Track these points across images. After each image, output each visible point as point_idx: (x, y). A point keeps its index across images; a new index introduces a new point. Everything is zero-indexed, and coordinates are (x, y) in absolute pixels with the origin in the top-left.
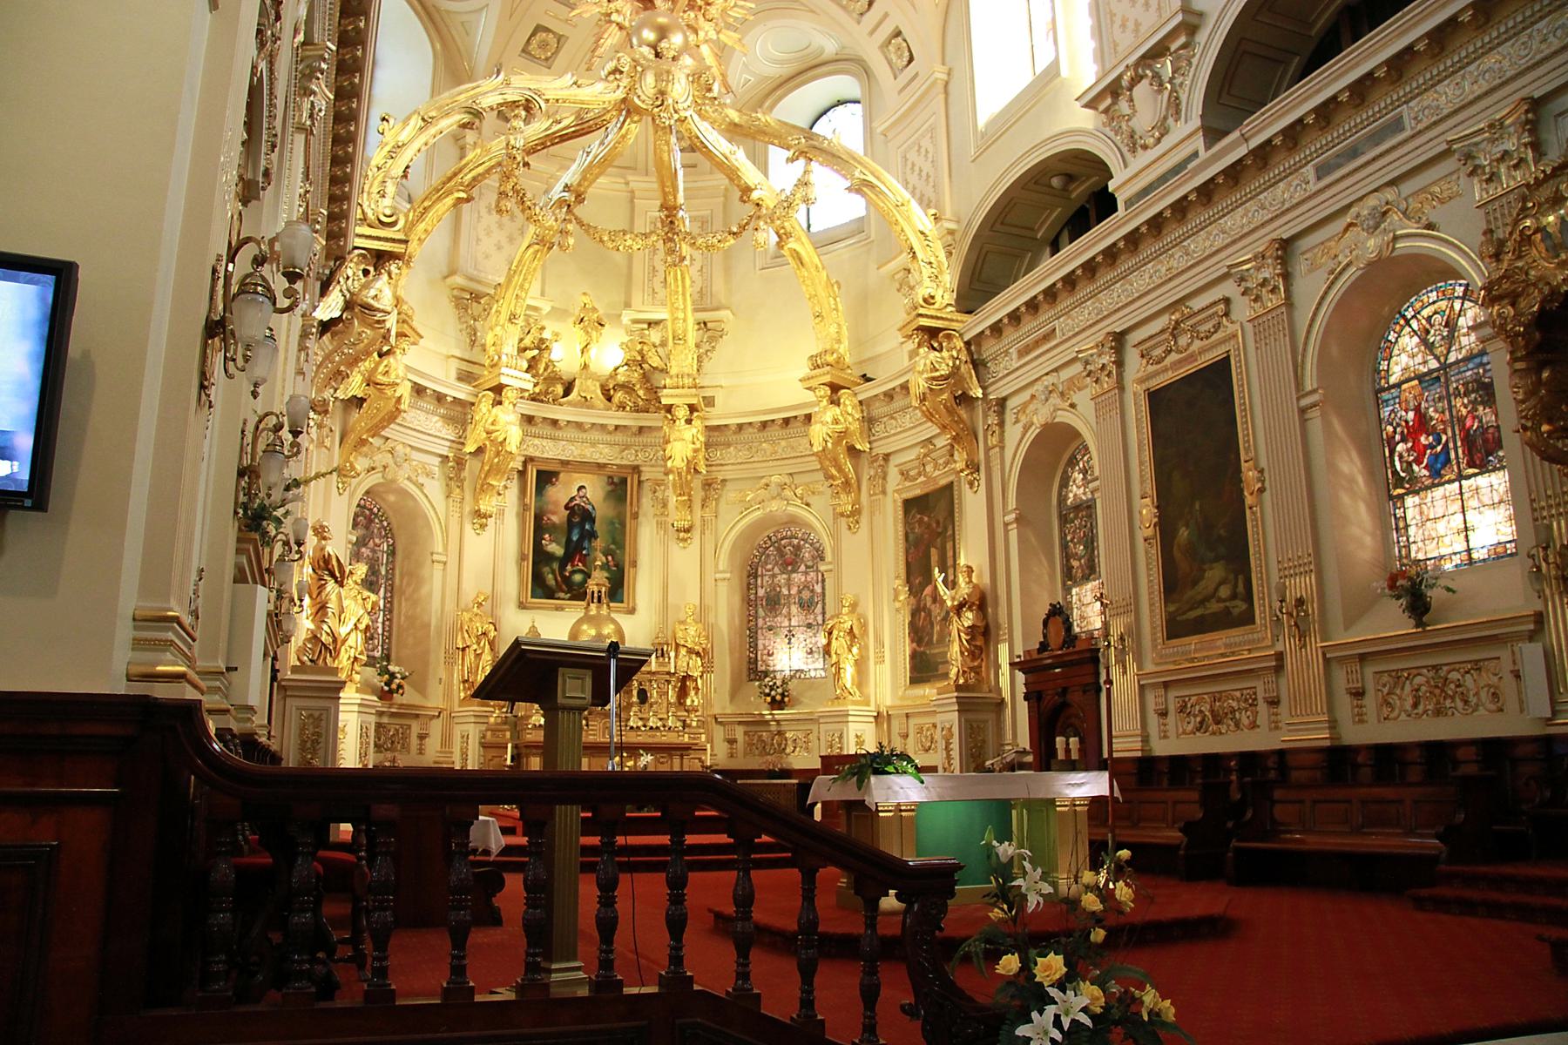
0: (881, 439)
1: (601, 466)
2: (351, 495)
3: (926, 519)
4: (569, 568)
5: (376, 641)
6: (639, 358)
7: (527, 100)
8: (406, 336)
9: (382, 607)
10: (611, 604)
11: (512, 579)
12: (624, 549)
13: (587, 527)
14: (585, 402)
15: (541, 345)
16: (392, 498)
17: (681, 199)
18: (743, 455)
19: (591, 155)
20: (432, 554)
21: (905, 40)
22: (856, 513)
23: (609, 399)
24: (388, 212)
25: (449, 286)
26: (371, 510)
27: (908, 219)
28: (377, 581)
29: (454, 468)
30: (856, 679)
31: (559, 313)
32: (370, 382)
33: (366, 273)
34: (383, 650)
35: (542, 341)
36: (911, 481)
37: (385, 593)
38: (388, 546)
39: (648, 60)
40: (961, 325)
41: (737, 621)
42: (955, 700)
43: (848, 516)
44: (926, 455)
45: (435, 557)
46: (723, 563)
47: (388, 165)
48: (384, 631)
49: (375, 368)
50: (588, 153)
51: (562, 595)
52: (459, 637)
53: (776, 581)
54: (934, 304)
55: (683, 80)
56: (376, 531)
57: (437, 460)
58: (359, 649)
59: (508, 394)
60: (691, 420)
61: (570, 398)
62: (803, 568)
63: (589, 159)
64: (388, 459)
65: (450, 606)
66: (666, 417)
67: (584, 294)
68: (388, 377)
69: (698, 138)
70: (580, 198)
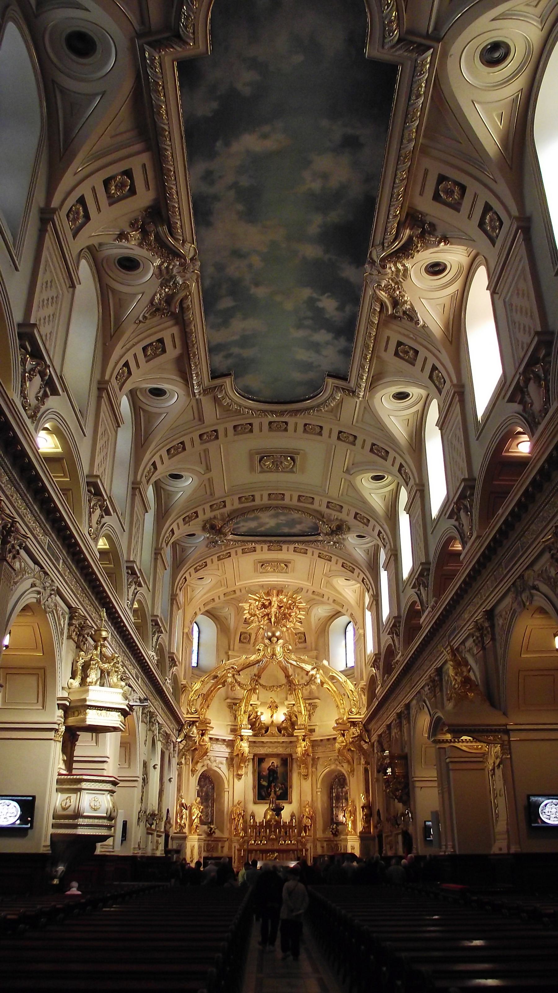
11: (250, 795)
15: (257, 717)
22: (352, 771)
23: (280, 732)
31: (263, 704)
35: (257, 716)
41: (326, 805)
59: (246, 738)
64: (209, 762)
70: (259, 677)
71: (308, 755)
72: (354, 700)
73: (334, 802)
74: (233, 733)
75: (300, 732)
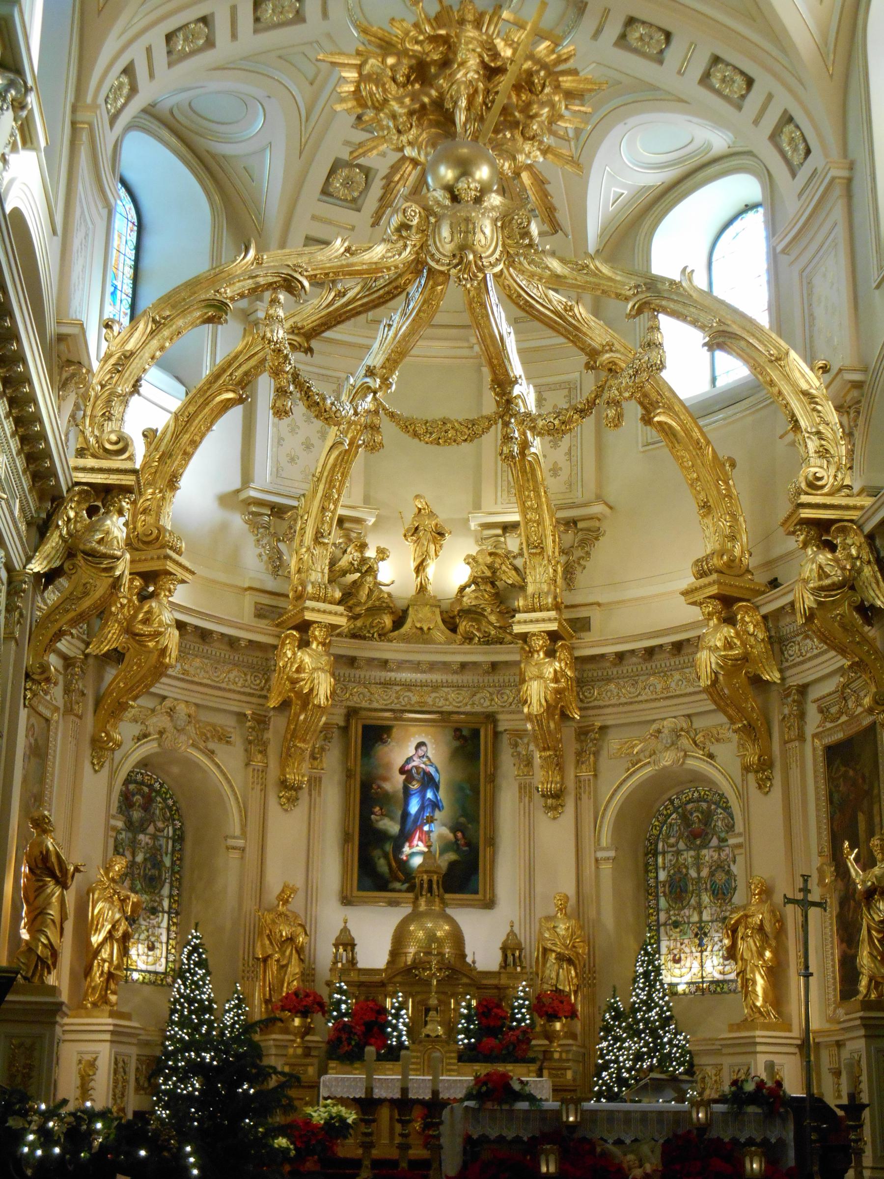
0: (795, 665)
1: (444, 717)
2: (113, 774)
3: (851, 773)
4: (406, 850)
5: (158, 952)
6: (488, 573)
7: (285, 280)
8: (171, 574)
9: (166, 908)
10: (447, 896)
12: (478, 822)
13: (429, 795)
14: (422, 635)
16: (175, 770)
17: (517, 368)
18: (627, 692)
19: (393, 329)
20: (226, 838)
21: (797, 127)
22: (764, 766)
23: (454, 629)
24: (114, 438)
25: (243, 501)
26: (150, 786)
27: (787, 378)
28: (160, 876)
29: (253, 728)
30: (771, 996)
32: (129, 630)
33: (92, 511)
34: (167, 962)
35: (364, 560)
36: (832, 721)
37: (172, 887)
38: (175, 830)
39: (446, 207)
40: (858, 513)
42: (858, 1022)
43: (757, 772)
44: (845, 686)
45: (231, 842)
46: (605, 839)
47: (114, 380)
48: (168, 939)
49: (135, 616)
50: (390, 326)
51: (398, 885)
52: (259, 944)
53: (681, 860)
54: (822, 487)
55: (488, 230)
56: (157, 812)
57: (229, 722)
58: (115, 962)
60: (555, 651)
61: (403, 630)
62: (715, 842)
63: (391, 333)
65: (250, 905)
66: (523, 648)
67: (417, 497)
68: (150, 625)
69: (520, 296)
71: (564, 716)
72: (818, 433)
73: (663, 902)
74: (263, 624)
75: (537, 621)
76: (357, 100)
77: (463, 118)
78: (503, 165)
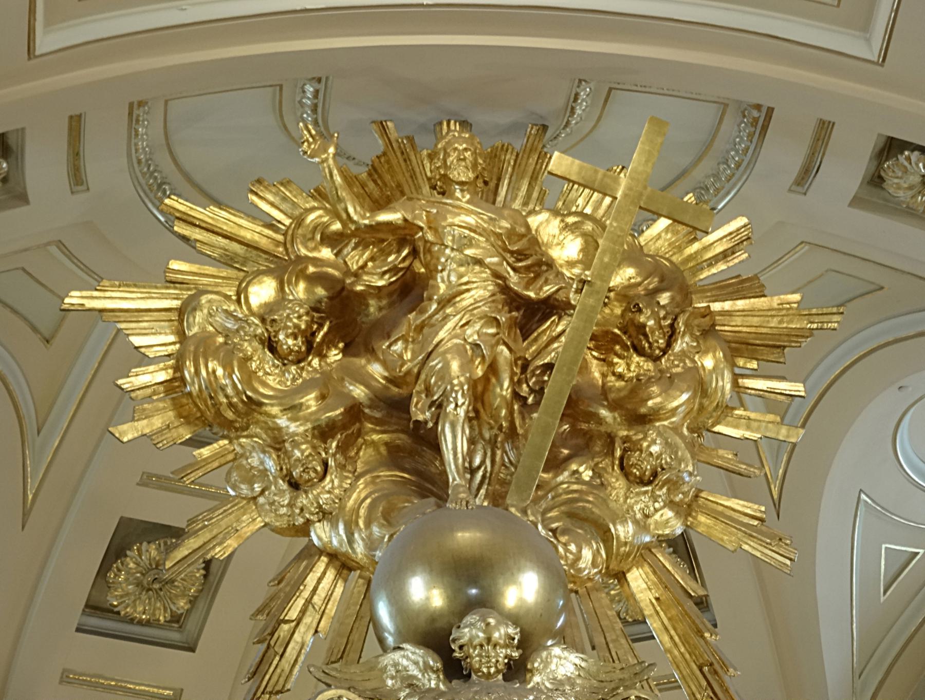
76: (177, 407)
77: (463, 445)
78: (578, 558)
